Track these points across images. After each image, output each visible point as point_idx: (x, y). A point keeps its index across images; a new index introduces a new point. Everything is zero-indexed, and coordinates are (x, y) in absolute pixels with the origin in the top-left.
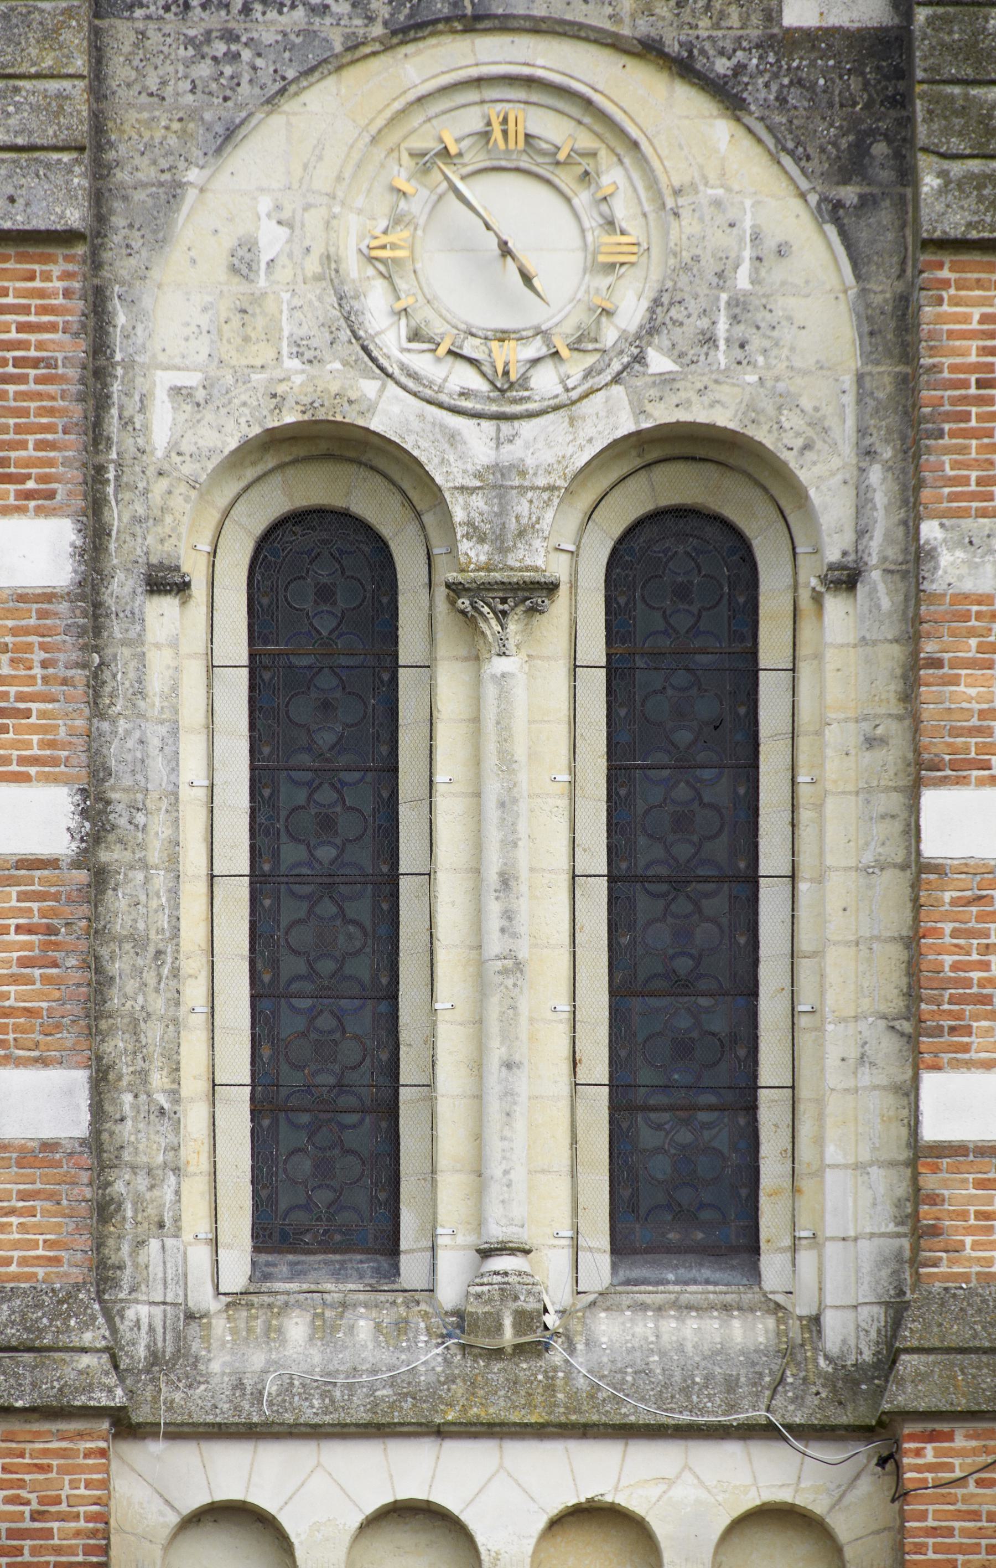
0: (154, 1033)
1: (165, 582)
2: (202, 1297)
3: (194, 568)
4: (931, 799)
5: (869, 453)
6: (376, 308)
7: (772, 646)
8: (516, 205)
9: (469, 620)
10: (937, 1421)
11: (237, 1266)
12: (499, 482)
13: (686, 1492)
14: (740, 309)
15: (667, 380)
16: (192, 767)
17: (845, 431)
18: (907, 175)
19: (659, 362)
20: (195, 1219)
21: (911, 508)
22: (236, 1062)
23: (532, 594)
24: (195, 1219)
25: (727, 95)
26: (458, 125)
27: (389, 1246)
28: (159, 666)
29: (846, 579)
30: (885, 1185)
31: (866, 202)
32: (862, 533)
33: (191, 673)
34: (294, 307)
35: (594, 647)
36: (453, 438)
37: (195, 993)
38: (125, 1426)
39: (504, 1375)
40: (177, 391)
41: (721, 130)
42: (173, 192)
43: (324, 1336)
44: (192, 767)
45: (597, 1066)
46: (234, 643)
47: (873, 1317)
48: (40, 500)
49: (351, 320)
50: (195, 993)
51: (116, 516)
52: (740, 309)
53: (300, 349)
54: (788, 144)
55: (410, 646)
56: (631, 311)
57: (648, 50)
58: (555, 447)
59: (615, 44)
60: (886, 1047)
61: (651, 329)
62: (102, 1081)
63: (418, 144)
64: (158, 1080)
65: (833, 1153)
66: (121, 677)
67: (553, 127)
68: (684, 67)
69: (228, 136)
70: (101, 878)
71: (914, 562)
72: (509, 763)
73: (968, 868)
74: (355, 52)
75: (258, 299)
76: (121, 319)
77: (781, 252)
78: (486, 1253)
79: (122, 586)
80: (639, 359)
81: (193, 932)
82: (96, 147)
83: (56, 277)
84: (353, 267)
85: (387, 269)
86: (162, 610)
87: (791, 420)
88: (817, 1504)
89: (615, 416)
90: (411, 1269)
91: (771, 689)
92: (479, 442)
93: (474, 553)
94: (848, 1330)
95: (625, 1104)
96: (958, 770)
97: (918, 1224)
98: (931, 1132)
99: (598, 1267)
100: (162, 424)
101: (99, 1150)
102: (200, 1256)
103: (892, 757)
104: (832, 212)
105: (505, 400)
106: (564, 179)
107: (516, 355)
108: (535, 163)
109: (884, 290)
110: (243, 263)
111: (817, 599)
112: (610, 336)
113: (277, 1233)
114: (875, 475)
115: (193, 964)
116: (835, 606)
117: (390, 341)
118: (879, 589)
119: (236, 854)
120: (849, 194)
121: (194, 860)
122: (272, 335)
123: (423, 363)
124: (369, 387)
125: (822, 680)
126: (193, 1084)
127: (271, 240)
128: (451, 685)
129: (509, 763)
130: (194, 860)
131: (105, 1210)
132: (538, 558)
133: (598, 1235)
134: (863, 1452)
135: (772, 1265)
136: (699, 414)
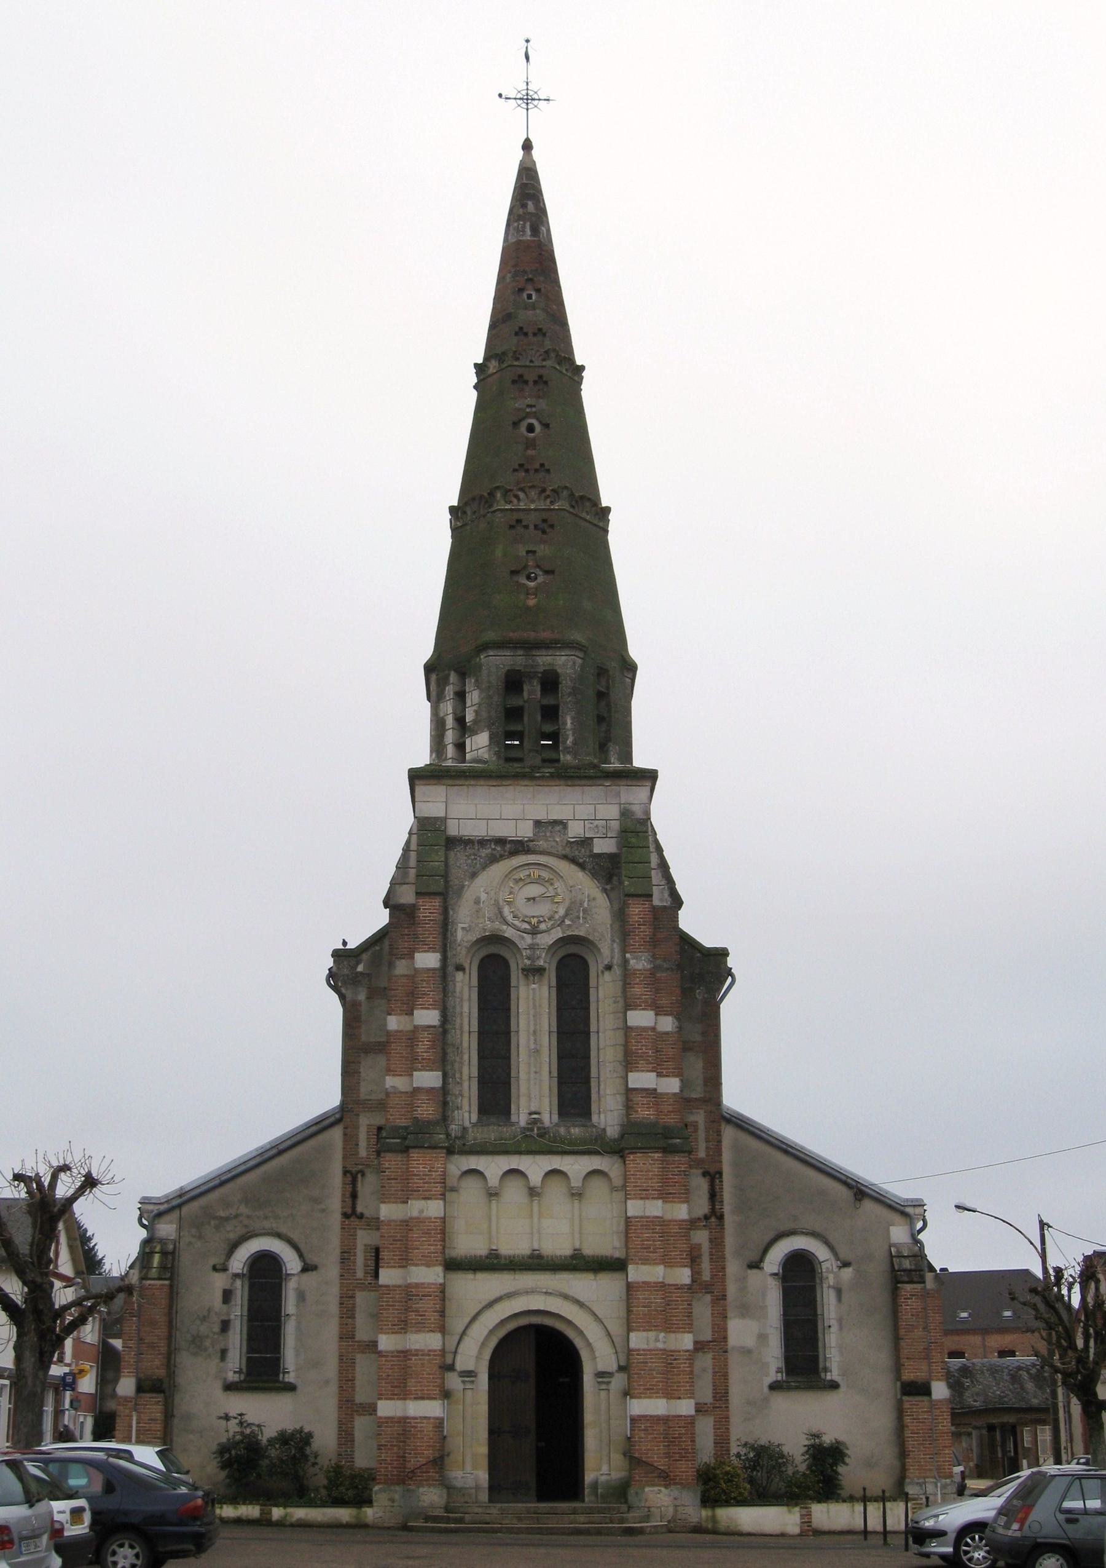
0: (456, 1065)
1: (460, 968)
2: (467, 1124)
3: (467, 967)
4: (629, 1013)
5: (613, 941)
6: (506, 910)
7: (592, 982)
8: (534, 890)
9: (526, 976)
10: (634, 1150)
11: (475, 1117)
12: (532, 947)
13: (576, 1167)
14: (585, 911)
15: (569, 926)
16: (466, 1009)
17: (608, 937)
18: (621, 883)
19: (568, 922)
20: (466, 1107)
21: (624, 951)
22: (475, 1072)
23: (540, 971)
24: (466, 1107)
25: (582, 866)
26: (522, 875)
27: (507, 1112)
28: (459, 985)
29: (609, 968)
30: (620, 1099)
31: (612, 889)
32: (612, 958)
33: (466, 989)
34: (488, 911)
35: (554, 983)
36: (523, 938)
37: (466, 1057)
38: (450, 1152)
39: (537, 1141)
40: (463, 928)
41: (580, 875)
42: (463, 887)
43: (492, 1133)
44: (466, 1009)
45: (555, 1074)
46: (475, 981)
47: (617, 1129)
48: (433, 949)
49: (501, 913)
50: (466, 1057)
51: (449, 954)
52: (585, 911)
53: (490, 919)
54: (594, 875)
55: (513, 983)
56: (562, 911)
57: (565, 857)
58: (546, 940)
59: (558, 856)
60: (620, 1069)
61: (567, 915)
62: (445, 1076)
63: (516, 877)
64: (457, 1075)
65: (608, 1092)
66: (450, 987)
67: (545, 874)
68: (573, 861)
69: (474, 875)
70: (445, 1032)
71: (625, 962)
72: (533, 1009)
73: (637, 1028)
74: (502, 857)
75: (480, 909)
76: (451, 913)
77: (594, 899)
78: (530, 1114)
79: (450, 969)
80: (563, 921)
81: (465, 1044)
82: (446, 876)
83: (437, 902)
84: (501, 902)
85: (509, 903)
86: (459, 976)
87: (596, 934)
88: (606, 1170)
89: (557, 934)
90: (514, 1118)
91: (592, 991)
92: (528, 939)
93: (528, 962)
94: (613, 1131)
95: (561, 1083)
96: (635, 1007)
97: (629, 1106)
98: (630, 1086)
99: (555, 1118)
100: (460, 934)
101: (444, 1090)
102: (466, 1115)
103: (621, 1004)
104: (605, 891)
105: (534, 932)
106: (547, 884)
107: (534, 921)
108: (539, 881)
109: (616, 907)
110: (477, 901)
111: (603, 972)
112: (557, 917)
113: (483, 1110)
114: (615, 945)
115: (466, 1051)
116: (607, 974)
117: (510, 918)
118: (617, 971)
119: (475, 1027)
120: (608, 887)
121: (466, 1028)
122: (484, 917)
123: (516, 923)
124: (505, 927)
125: (604, 991)
126: (465, 1077)
127: (483, 897)
128: (523, 990)
129: (533, 1009)
130: (466, 1028)
131: (445, 1104)
132: (541, 963)
133: (555, 1111)
134: (616, 1158)
135: (595, 1118)
136: (576, 933)
